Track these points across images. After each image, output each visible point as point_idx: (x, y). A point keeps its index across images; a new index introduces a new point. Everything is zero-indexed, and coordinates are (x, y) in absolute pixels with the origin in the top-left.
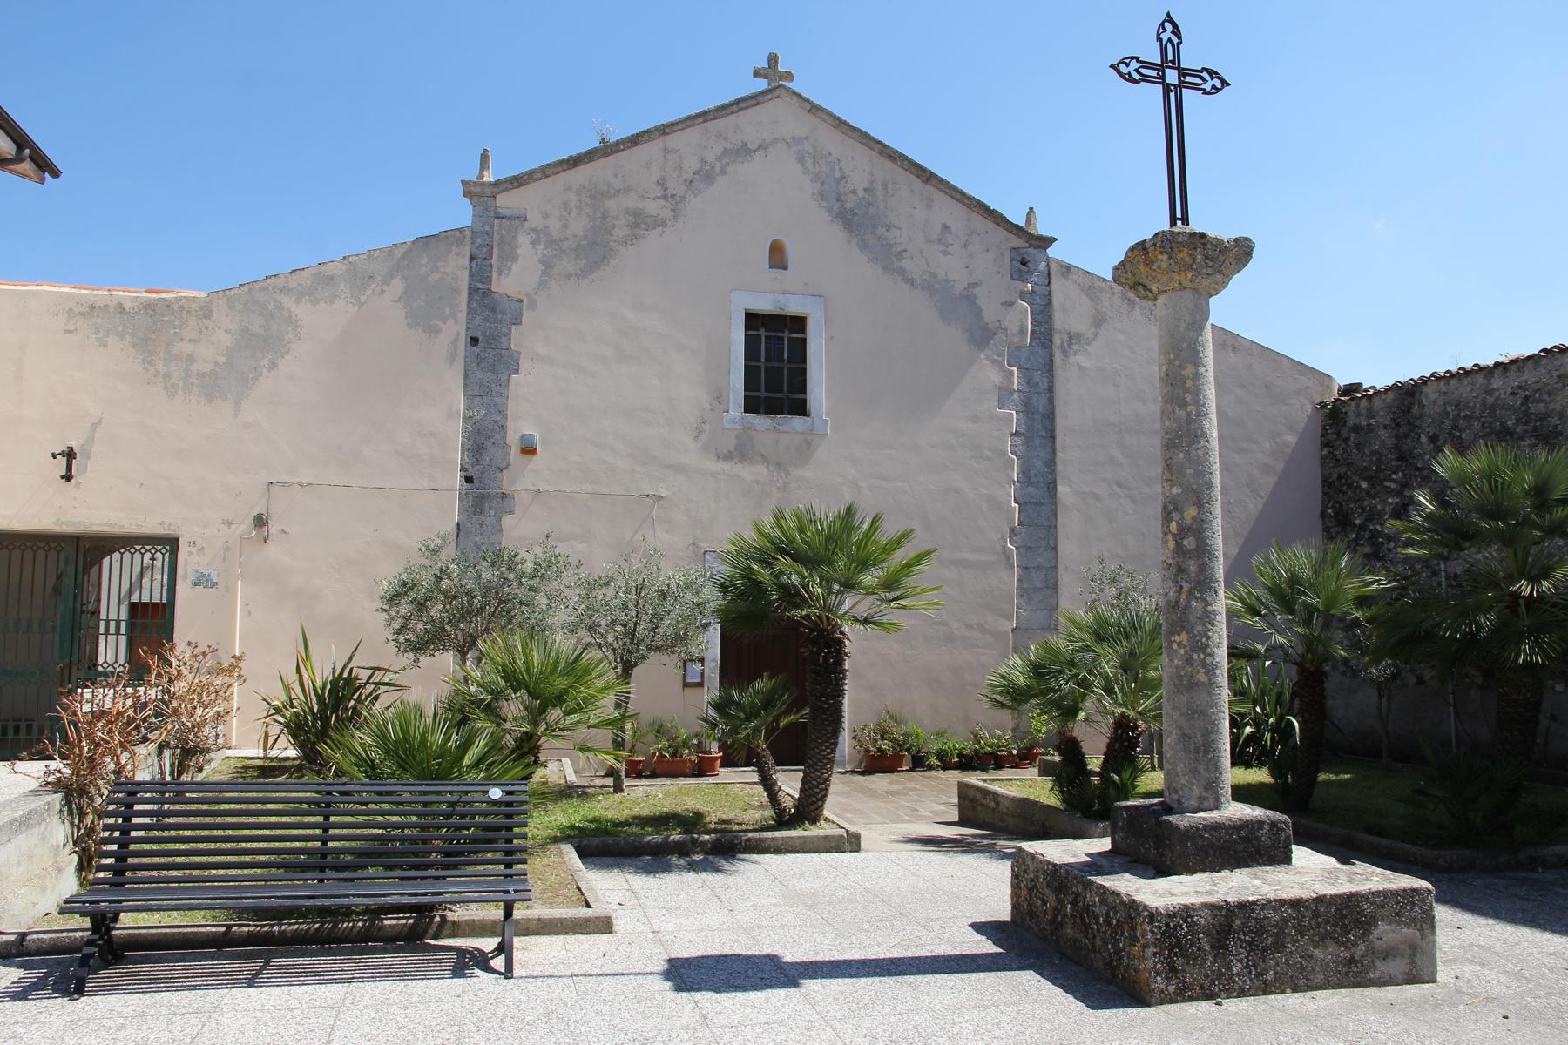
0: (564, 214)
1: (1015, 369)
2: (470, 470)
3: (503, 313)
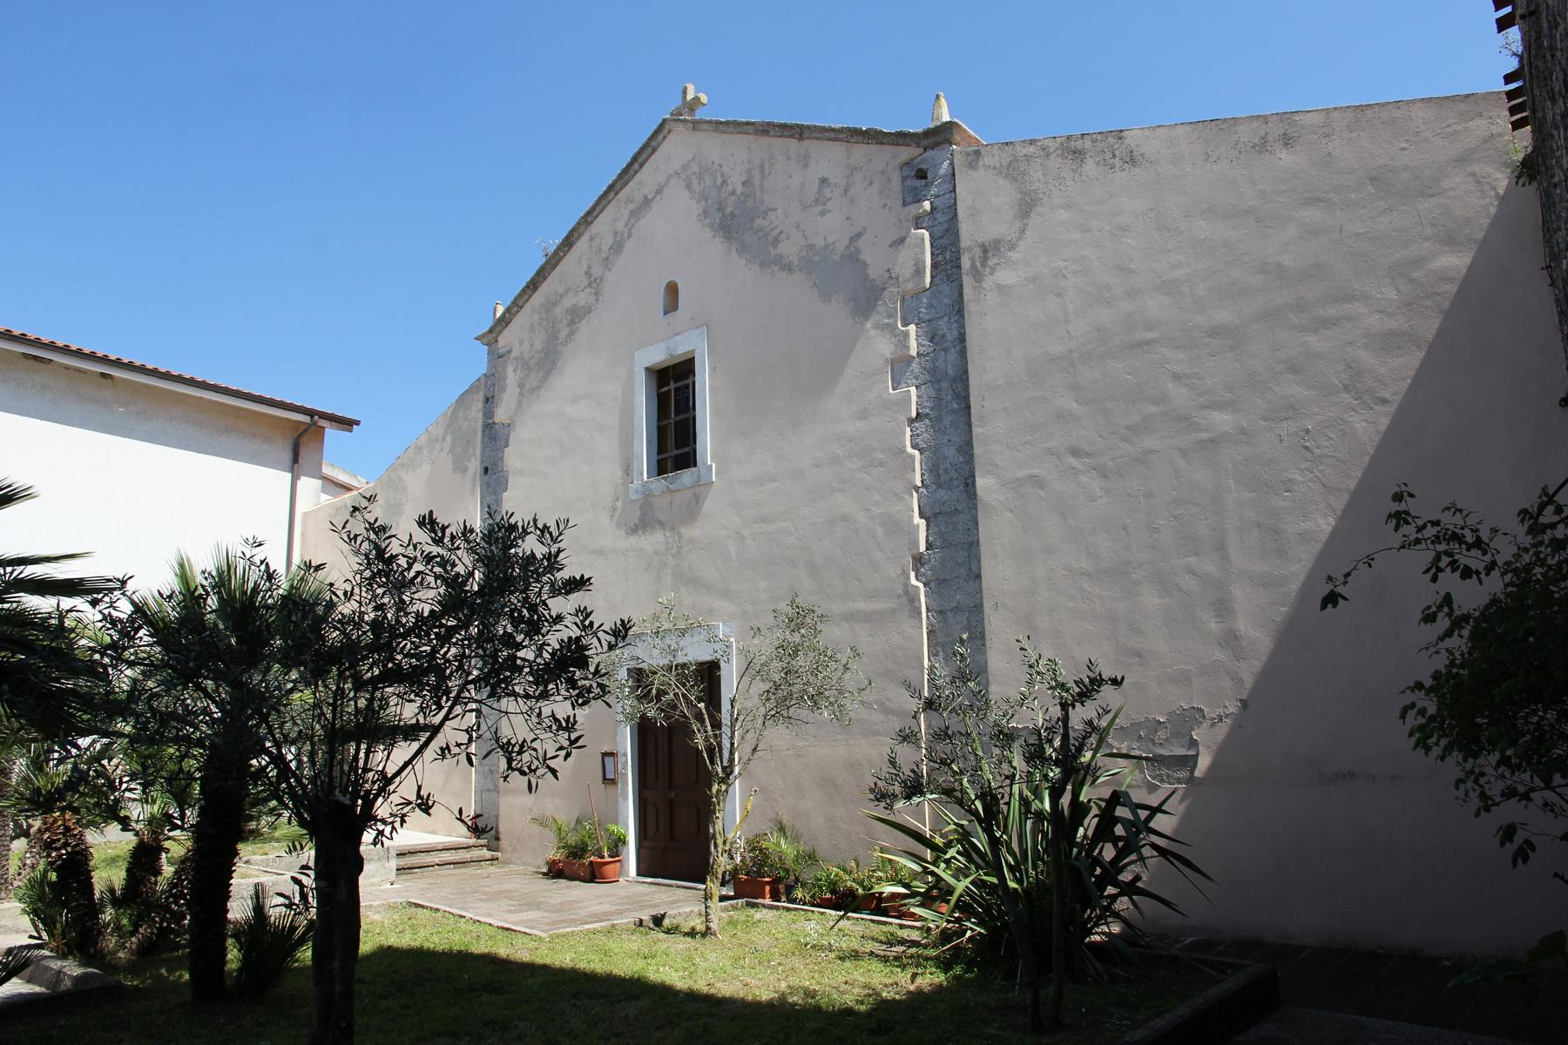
1: (912, 328)
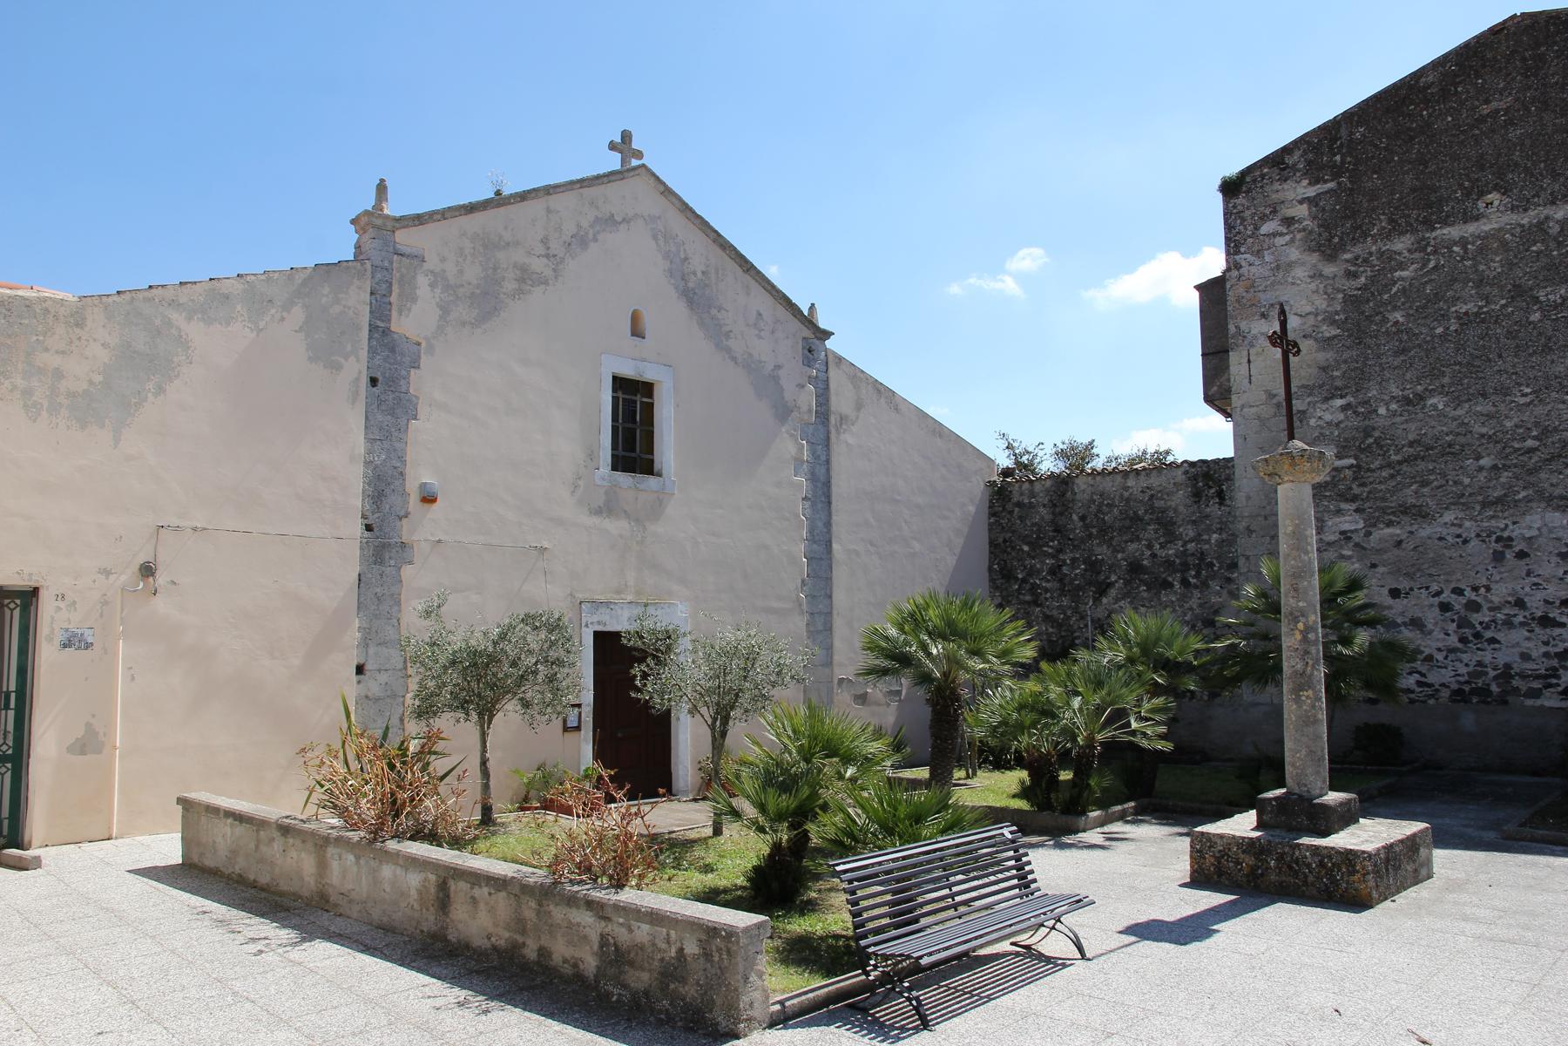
0: (460, 260)
2: (371, 517)
3: (402, 354)
